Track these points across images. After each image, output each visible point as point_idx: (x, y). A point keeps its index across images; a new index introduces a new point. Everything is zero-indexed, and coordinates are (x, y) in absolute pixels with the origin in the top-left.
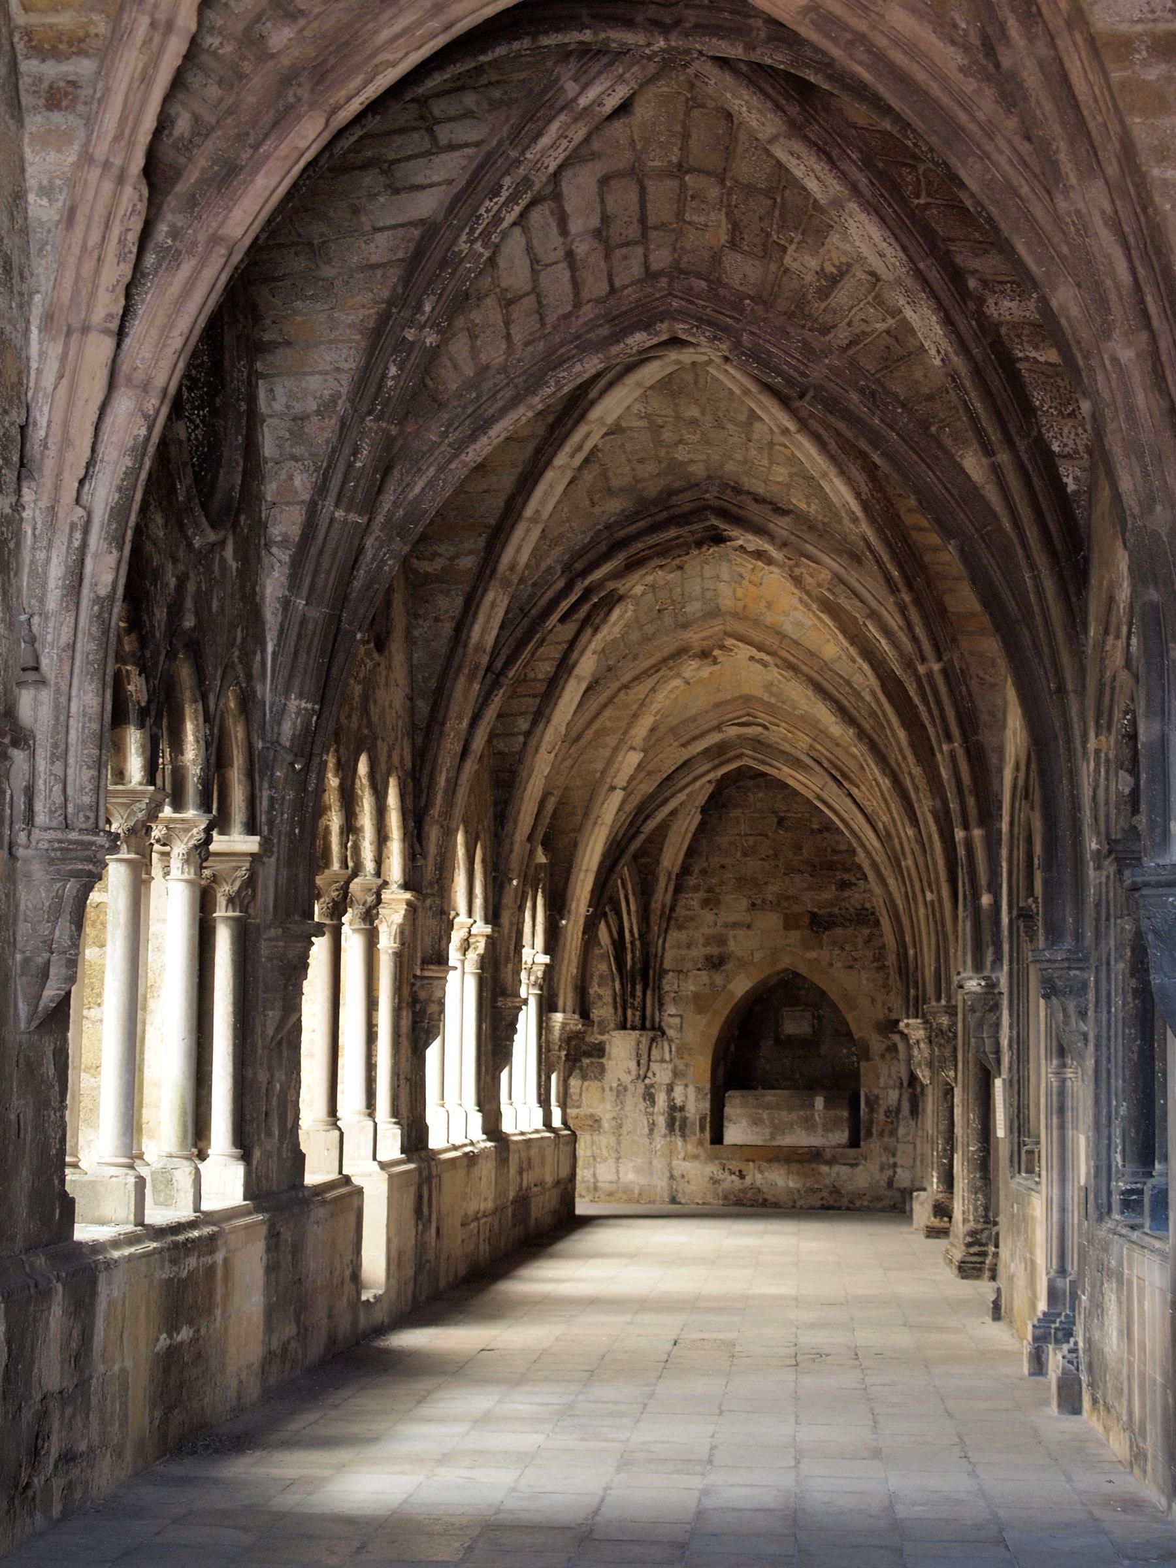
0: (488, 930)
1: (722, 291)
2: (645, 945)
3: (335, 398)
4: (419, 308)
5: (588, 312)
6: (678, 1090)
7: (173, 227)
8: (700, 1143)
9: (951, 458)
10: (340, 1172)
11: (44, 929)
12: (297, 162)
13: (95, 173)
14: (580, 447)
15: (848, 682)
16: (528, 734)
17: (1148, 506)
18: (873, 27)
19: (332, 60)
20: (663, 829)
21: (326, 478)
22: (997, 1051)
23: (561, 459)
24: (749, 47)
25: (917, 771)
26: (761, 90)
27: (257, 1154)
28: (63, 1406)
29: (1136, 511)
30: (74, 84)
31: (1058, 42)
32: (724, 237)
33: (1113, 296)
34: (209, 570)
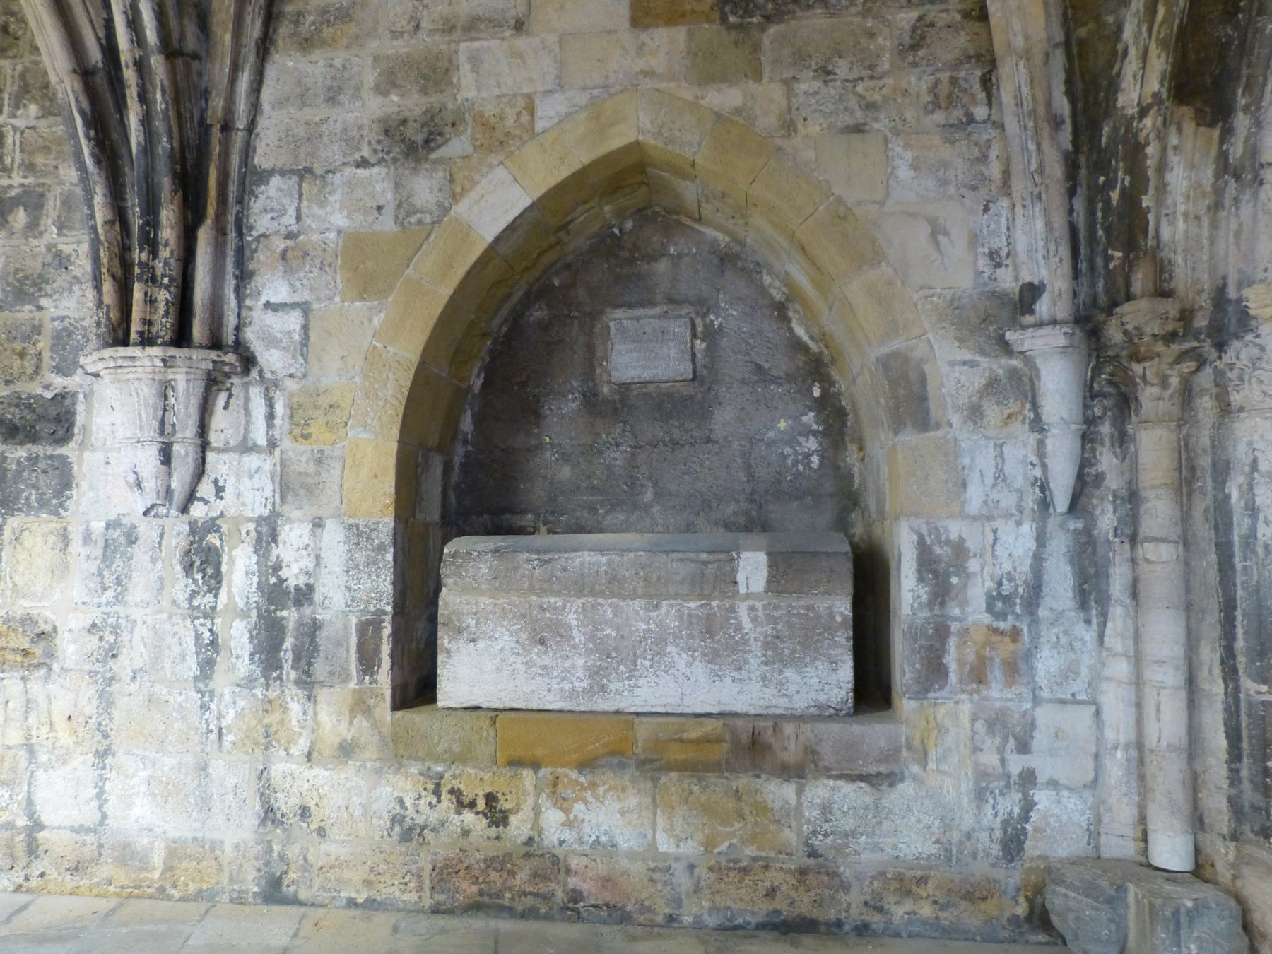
6: (294, 535)
8: (360, 706)
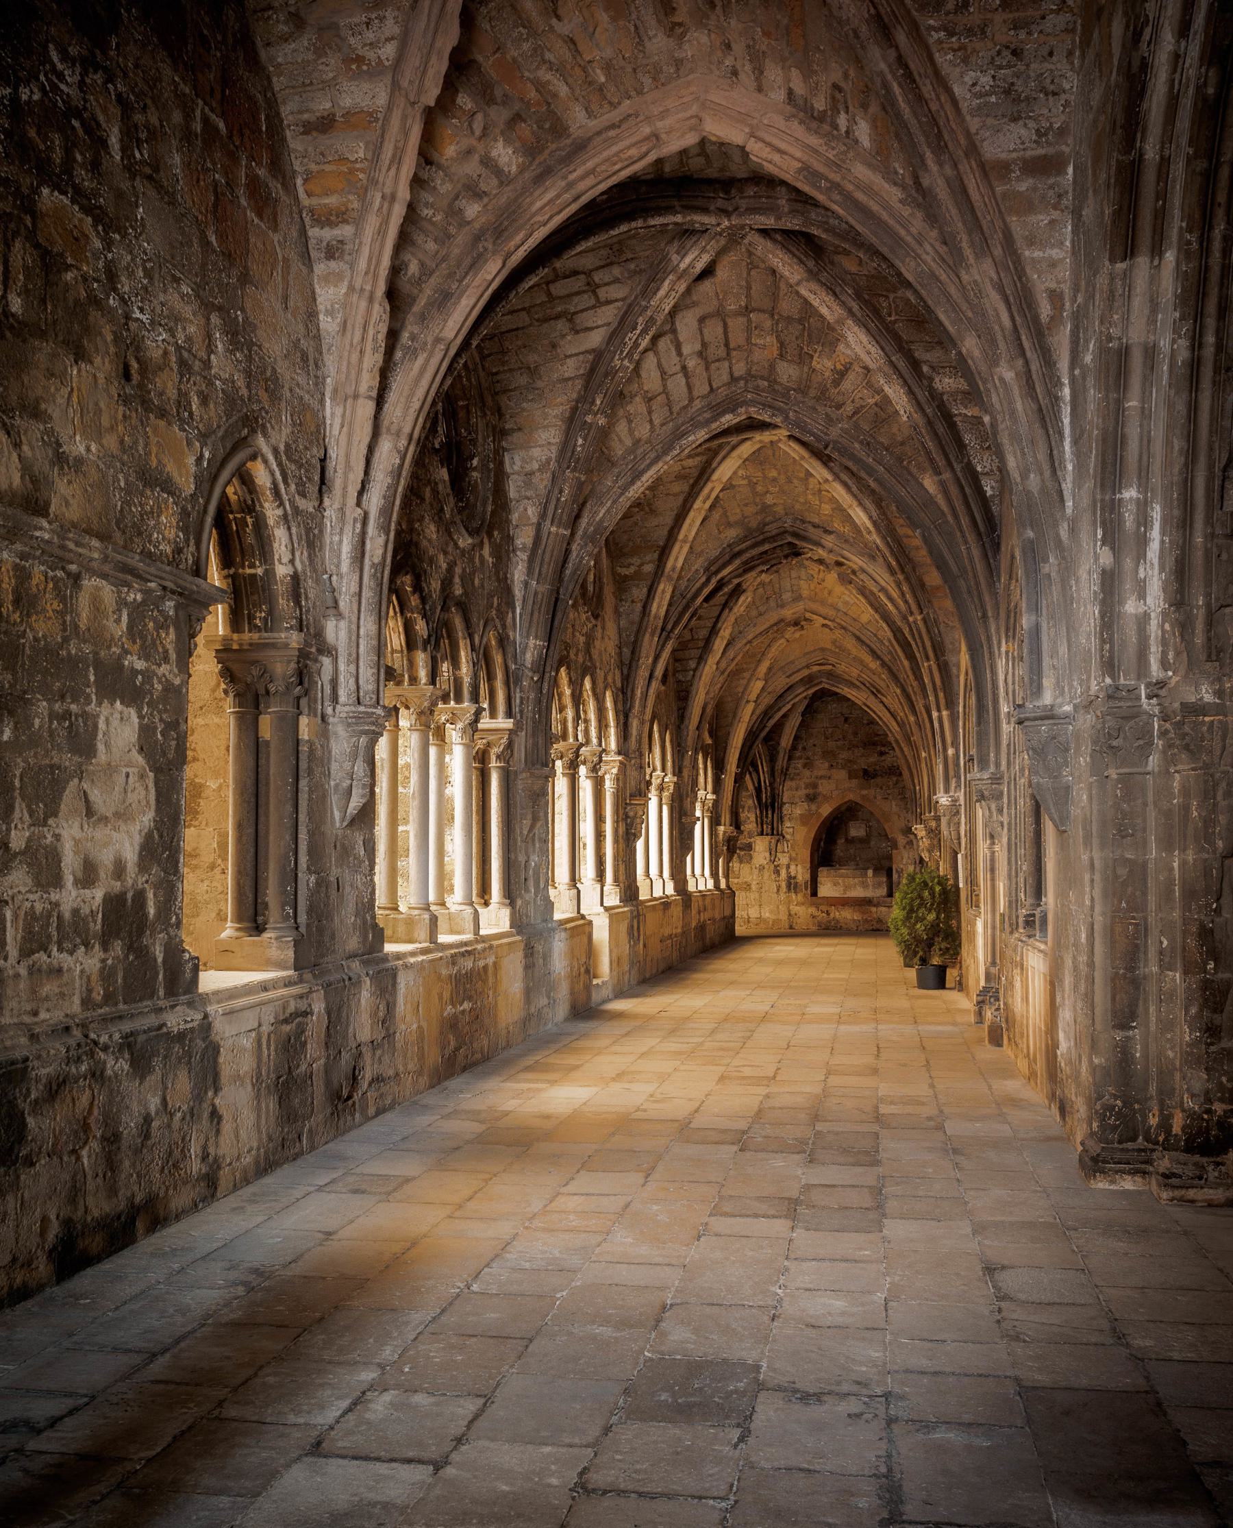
0: (675, 779)
1: (776, 387)
2: (773, 789)
3: (548, 461)
4: (593, 402)
5: (698, 404)
6: (793, 867)
7: (412, 333)
9: (916, 480)
10: (579, 912)
11: (347, 765)
12: (485, 290)
13: (355, 298)
14: (708, 497)
15: (875, 635)
16: (695, 670)
17: (1024, 476)
18: (844, 178)
19: (506, 223)
20: (779, 726)
21: (545, 508)
22: (959, 838)
23: (698, 504)
24: (779, 218)
25: (915, 684)
26: (791, 252)
27: (519, 902)
28: (374, 1050)
29: (1018, 480)
30: (341, 242)
31: (960, 167)
32: (776, 353)
33: (999, 337)
34: (471, 560)
